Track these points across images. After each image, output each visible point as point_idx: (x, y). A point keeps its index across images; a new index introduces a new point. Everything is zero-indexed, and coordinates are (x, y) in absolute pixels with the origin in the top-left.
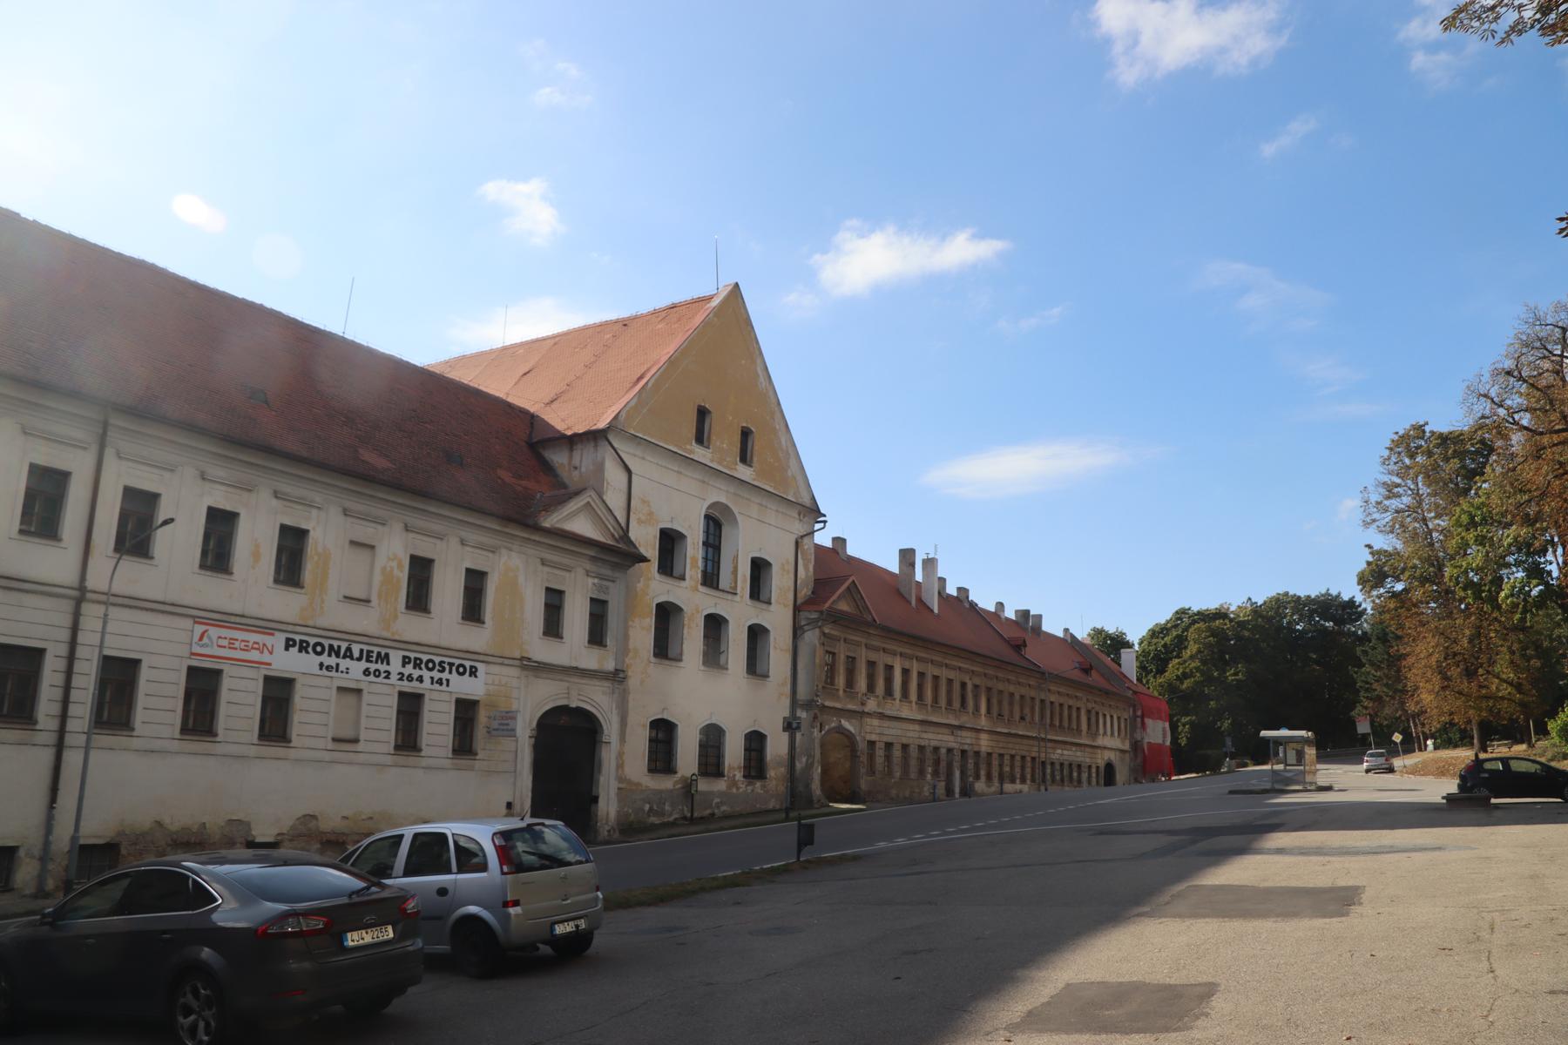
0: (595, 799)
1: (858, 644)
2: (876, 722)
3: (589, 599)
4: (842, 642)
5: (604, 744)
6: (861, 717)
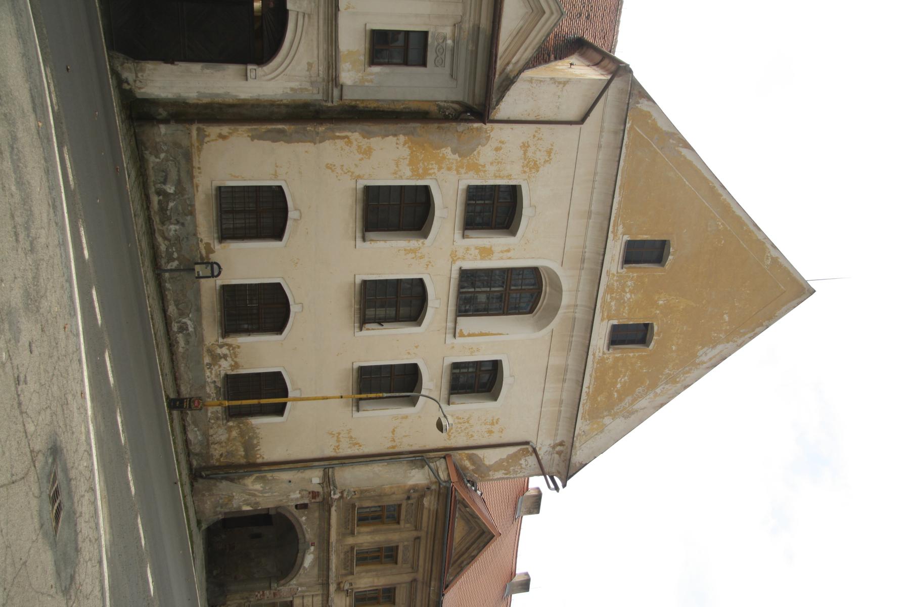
4: (415, 534)
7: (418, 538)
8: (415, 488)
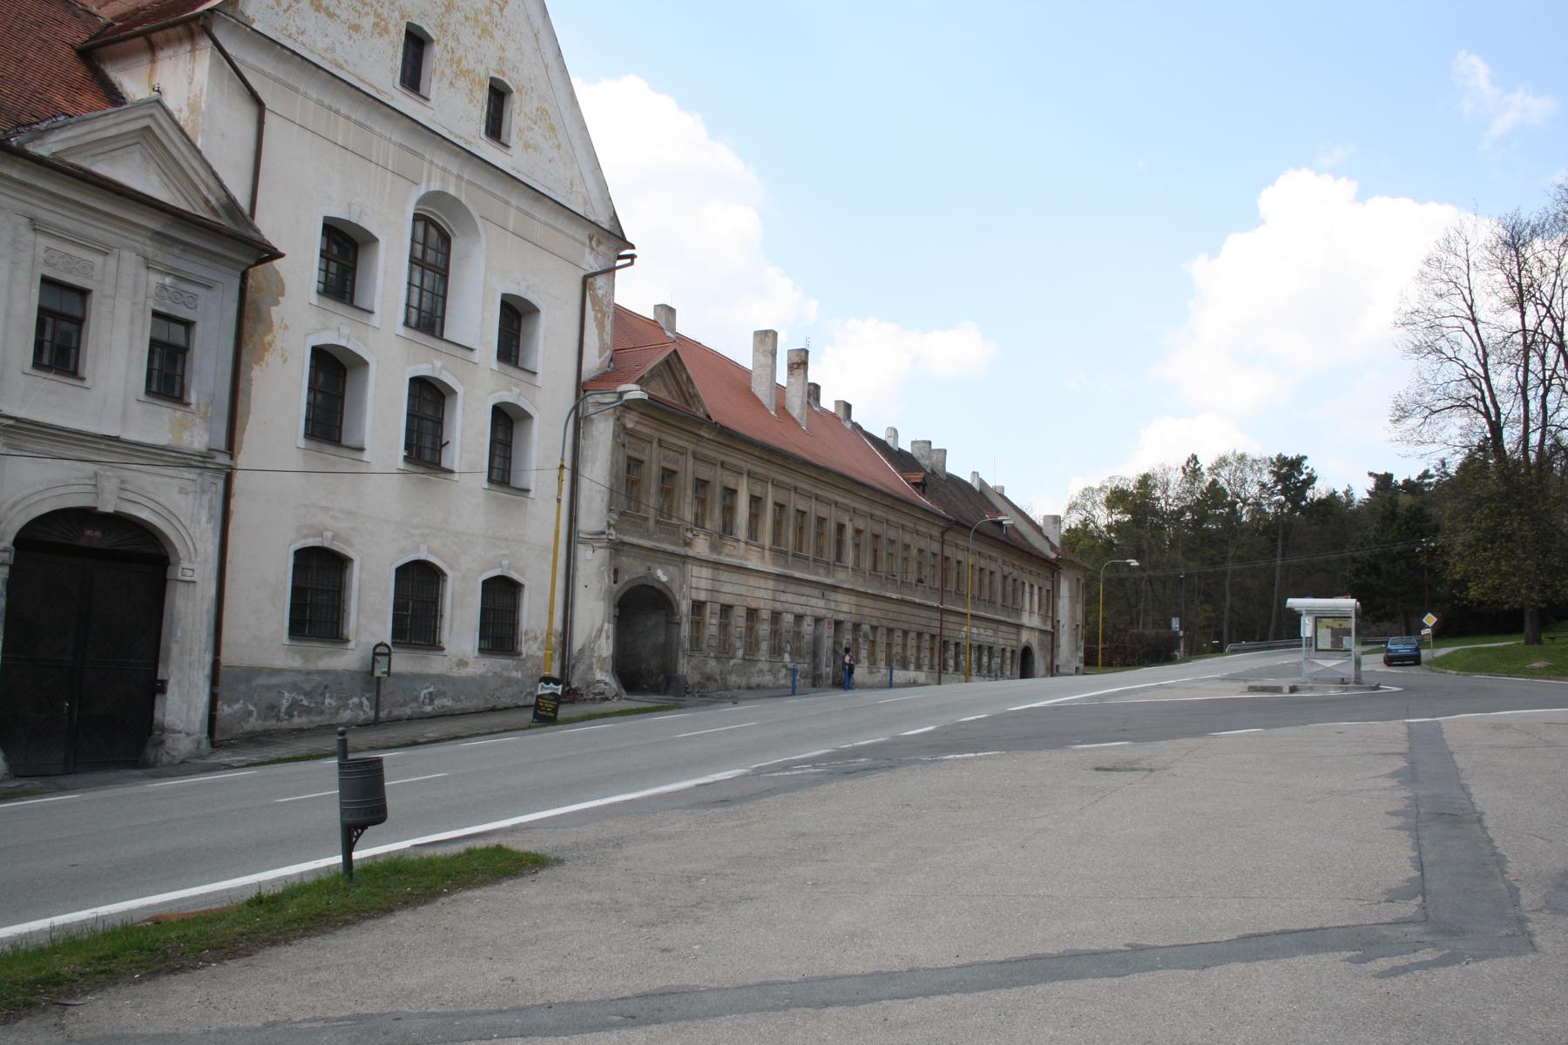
0: (161, 687)
1: (682, 451)
2: (706, 572)
3: (150, 313)
4: (655, 444)
5: (179, 584)
6: (684, 563)
7: (660, 441)
8: (615, 436)
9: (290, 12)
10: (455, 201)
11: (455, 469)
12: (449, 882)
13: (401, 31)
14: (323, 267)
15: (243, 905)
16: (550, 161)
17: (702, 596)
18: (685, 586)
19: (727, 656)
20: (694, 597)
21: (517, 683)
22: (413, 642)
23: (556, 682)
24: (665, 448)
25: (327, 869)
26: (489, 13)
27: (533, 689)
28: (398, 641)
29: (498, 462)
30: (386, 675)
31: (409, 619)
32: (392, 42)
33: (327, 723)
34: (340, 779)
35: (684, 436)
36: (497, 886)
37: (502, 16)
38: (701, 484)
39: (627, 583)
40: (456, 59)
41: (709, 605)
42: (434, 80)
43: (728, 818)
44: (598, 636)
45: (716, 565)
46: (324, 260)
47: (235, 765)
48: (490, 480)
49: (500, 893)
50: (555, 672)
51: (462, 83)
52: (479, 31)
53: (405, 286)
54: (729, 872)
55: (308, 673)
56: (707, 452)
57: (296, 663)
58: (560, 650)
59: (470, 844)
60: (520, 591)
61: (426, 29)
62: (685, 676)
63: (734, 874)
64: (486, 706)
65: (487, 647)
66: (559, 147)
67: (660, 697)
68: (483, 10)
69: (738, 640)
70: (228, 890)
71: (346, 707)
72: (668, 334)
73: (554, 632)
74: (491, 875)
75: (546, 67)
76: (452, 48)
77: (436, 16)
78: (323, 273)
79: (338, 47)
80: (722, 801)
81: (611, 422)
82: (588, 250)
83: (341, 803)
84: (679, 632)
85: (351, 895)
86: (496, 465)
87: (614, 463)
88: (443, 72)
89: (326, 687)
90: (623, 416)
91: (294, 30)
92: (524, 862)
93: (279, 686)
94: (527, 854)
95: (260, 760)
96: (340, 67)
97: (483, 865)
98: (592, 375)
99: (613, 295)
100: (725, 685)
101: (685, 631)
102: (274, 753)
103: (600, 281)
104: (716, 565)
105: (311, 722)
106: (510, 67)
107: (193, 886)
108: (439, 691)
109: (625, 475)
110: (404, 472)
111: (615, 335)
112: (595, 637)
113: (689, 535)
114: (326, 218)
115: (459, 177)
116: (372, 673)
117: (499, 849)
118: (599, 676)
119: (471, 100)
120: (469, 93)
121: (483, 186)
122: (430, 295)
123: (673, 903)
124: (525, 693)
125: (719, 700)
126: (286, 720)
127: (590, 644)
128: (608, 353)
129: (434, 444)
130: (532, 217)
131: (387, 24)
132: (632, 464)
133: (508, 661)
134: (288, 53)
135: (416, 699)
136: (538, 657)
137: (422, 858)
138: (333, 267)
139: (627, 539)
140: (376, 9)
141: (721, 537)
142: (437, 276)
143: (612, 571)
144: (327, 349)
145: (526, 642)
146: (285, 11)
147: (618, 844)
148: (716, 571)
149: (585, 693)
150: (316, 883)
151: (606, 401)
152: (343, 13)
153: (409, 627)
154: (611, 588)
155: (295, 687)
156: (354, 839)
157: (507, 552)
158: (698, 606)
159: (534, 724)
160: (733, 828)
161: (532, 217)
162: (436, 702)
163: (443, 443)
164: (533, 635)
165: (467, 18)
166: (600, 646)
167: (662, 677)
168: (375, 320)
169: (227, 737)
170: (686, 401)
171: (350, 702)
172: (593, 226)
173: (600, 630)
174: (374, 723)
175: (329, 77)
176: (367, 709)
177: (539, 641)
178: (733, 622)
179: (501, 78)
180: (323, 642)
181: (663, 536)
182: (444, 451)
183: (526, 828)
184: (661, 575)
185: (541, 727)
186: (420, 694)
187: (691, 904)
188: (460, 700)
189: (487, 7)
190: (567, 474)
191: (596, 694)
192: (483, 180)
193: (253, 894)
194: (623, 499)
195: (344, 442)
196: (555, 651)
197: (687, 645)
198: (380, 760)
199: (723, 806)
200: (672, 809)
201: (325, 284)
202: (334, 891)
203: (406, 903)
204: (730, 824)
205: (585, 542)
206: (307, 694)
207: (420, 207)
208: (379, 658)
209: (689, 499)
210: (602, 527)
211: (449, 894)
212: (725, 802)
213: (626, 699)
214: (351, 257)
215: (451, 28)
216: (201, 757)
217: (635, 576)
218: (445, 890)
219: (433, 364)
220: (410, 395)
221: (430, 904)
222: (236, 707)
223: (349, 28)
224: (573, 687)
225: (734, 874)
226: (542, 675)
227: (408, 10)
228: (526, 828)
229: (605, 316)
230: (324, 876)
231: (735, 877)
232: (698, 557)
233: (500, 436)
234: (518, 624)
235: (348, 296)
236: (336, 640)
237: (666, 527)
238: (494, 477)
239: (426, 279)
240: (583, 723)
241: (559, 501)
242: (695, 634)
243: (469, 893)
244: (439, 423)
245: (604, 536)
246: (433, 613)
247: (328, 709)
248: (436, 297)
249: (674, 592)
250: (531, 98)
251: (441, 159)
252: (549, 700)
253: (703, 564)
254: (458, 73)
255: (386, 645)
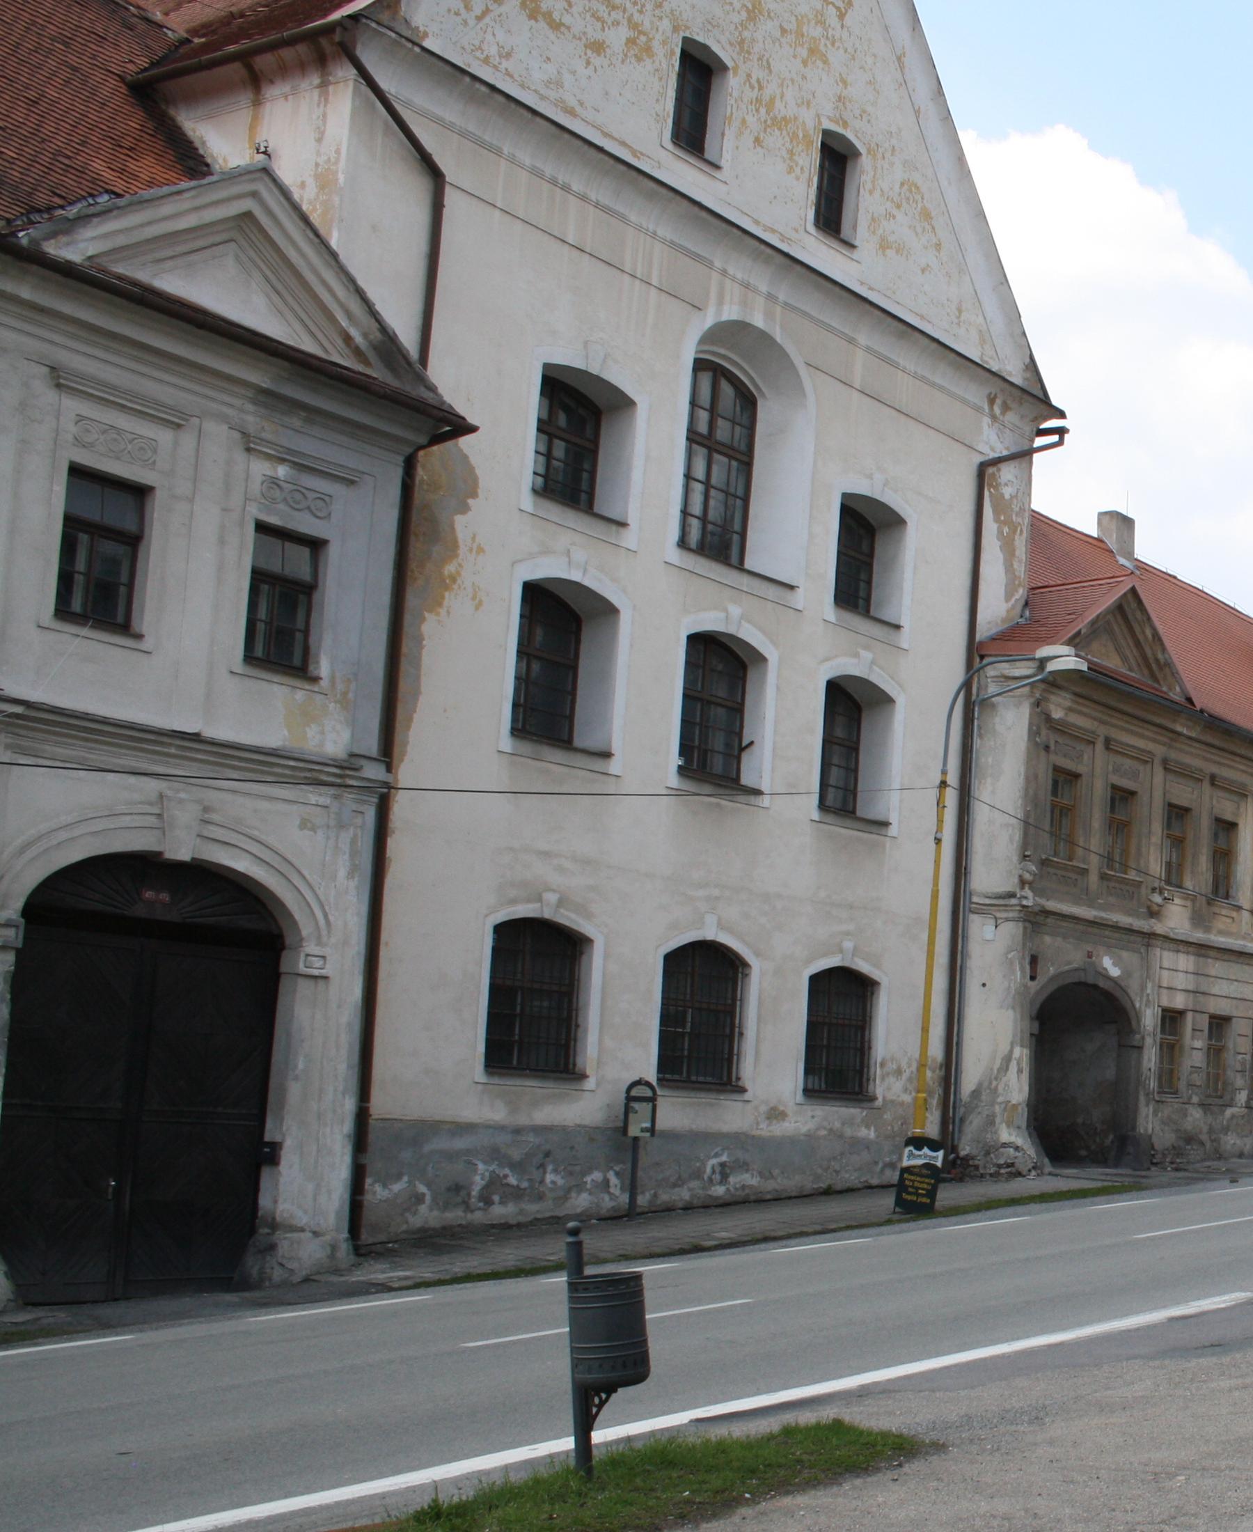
0: (270, 1155)
1: (1145, 758)
2: (1185, 962)
3: (252, 526)
4: (1100, 746)
5: (302, 983)
6: (1148, 945)
7: (1108, 741)
8: (1033, 733)
9: (487, 20)
10: (764, 338)
11: (763, 789)
12: (754, 1481)
13: (672, 53)
14: (543, 449)
15: (407, 1520)
16: (923, 271)
17: (1179, 1002)
18: (1149, 985)
19: (1220, 1102)
20: (1165, 1002)
21: (868, 1148)
22: (693, 1078)
23: (934, 1146)
24: (1117, 752)
25: (549, 1460)
26: (821, 22)
27: (895, 1157)
28: (668, 1076)
29: (835, 775)
30: (648, 1134)
31: (687, 1039)
32: (657, 70)
33: (548, 1214)
34: (571, 1308)
35: (1147, 733)
36: (835, 1489)
37: (842, 26)
38: (1177, 814)
39: (1052, 979)
40: (766, 98)
41: (1189, 1016)
42: (730, 135)
43: (1223, 1374)
44: (1005, 1068)
45: (1202, 949)
46: (545, 437)
47: (396, 1285)
48: (823, 806)
49: (840, 1500)
50: (932, 1129)
51: (776, 140)
52: (804, 53)
53: (679, 480)
54: (1223, 1464)
55: (518, 1131)
56: (1187, 760)
57: (497, 1113)
58: (941, 1091)
59: (789, 1418)
60: (872, 994)
61: (716, 49)
62: (1150, 1137)
63: (1232, 1469)
64: (815, 1186)
65: (817, 1087)
66: (938, 246)
67: (1108, 1171)
68: (811, 16)
69: (1238, 1075)
70: (383, 1496)
71: (580, 1187)
72: (1122, 561)
73: (929, 1063)
74: (824, 1471)
75: (917, 112)
76: (758, 81)
77: (733, 27)
78: (542, 459)
79: (567, 79)
80: (1212, 1345)
81: (1025, 710)
82: (987, 420)
83: (573, 1350)
84: (1139, 1061)
85: (590, 1503)
86: (832, 781)
87: (1031, 778)
88: (744, 121)
89: (547, 1154)
90: (1047, 700)
91: (493, 51)
92: (879, 1448)
93: (468, 1152)
94: (885, 1435)
95: (437, 1277)
96: (571, 112)
97: (812, 1454)
98: (994, 631)
99: (1030, 495)
100: (1216, 1151)
101: (1150, 1060)
102: (460, 1264)
103: (1007, 473)
104: (1202, 949)
105: (521, 1212)
106: (857, 112)
107: (323, 1489)
108: (737, 1160)
109: (1050, 797)
110: (677, 793)
111: (1032, 564)
112: (999, 1070)
113: (1157, 899)
114: (547, 367)
115: (771, 297)
116: (624, 1130)
117: (837, 1426)
118: (1006, 1135)
119: (791, 167)
120: (787, 156)
121: (813, 313)
122: (721, 496)
123: (1129, 1517)
124: (880, 1165)
125: (1207, 1176)
126: (479, 1209)
127: (990, 1083)
128: (1021, 593)
129: (728, 745)
130: (895, 365)
131: (650, 40)
132: (1061, 779)
133: (852, 1111)
134: (483, 89)
135: (698, 1175)
136: (902, 1104)
137: (708, 1441)
138: (559, 449)
139: (1052, 905)
140: (632, 15)
141: (1210, 903)
142: (734, 464)
143: (1027, 960)
144: (552, 588)
145: (883, 1079)
146: (479, 19)
147: (1037, 1418)
148: (1201, 959)
149: (981, 1163)
150: (531, 1483)
151: (1017, 673)
152: (576, 21)
153: (686, 1053)
154: (1025, 986)
155: (495, 1154)
156: (594, 1410)
157: (851, 927)
158: (1171, 1018)
159: (896, 1217)
160: (1230, 1390)
161: (895, 365)
162: (732, 1179)
163: (744, 744)
164: (895, 1067)
165: (784, 31)
166: (1007, 1085)
167: (1111, 1137)
168: (630, 538)
169: (382, 1238)
170: (1153, 676)
171: (588, 1179)
172: (996, 379)
173: (1008, 1059)
174: (629, 1215)
175: (553, 129)
176: (617, 1192)
177: (905, 1076)
178: (1230, 1045)
179: (840, 130)
180: (544, 1078)
181: (1112, 900)
182: (745, 757)
183: (883, 1392)
184: (1111, 967)
185: (907, 1221)
186: (704, 1165)
187: (1159, 1520)
188: (772, 1177)
189: (817, 11)
190: (951, 797)
191: (1000, 1166)
192: (811, 302)
193: (424, 1501)
194: (1046, 839)
195: (577, 742)
196: (931, 1094)
197: (1153, 1084)
198: (637, 1277)
199: (1213, 1355)
200: (1128, 1359)
201: (546, 477)
202: (561, 1497)
203: (682, 1517)
204: (1225, 1383)
205: (981, 910)
206: (518, 1167)
207: (706, 348)
208: (636, 1105)
209: (1156, 838)
210: (1011, 885)
211: (754, 1501)
212: (1217, 1347)
213: (1050, 1174)
214: (589, 432)
215: (757, 48)
216: (337, 1271)
217: (1067, 968)
218: (747, 1495)
219: (726, 610)
220: (688, 663)
221: (720, 1518)
222: (397, 1187)
223: (586, 46)
224: (962, 1153)
225: (1232, 1469)
226: (910, 1134)
227: (685, 16)
228: (883, 1392)
229: (1015, 532)
230: (544, 1472)
231: (1234, 1473)
232: (1172, 935)
233: (839, 732)
234: (870, 1048)
235: (583, 497)
236: (564, 1075)
237: (1117, 885)
238: (830, 801)
239: (715, 468)
240: (980, 1215)
241: (938, 841)
242: (1166, 1066)
243: (787, 1501)
244: (737, 710)
245: (1013, 901)
246: (728, 1031)
247: (551, 1190)
248: (731, 501)
249: (1132, 994)
250: (892, 164)
251: (741, 267)
252: (922, 1176)
253: (1181, 948)
254: (769, 122)
255: (648, 1084)
